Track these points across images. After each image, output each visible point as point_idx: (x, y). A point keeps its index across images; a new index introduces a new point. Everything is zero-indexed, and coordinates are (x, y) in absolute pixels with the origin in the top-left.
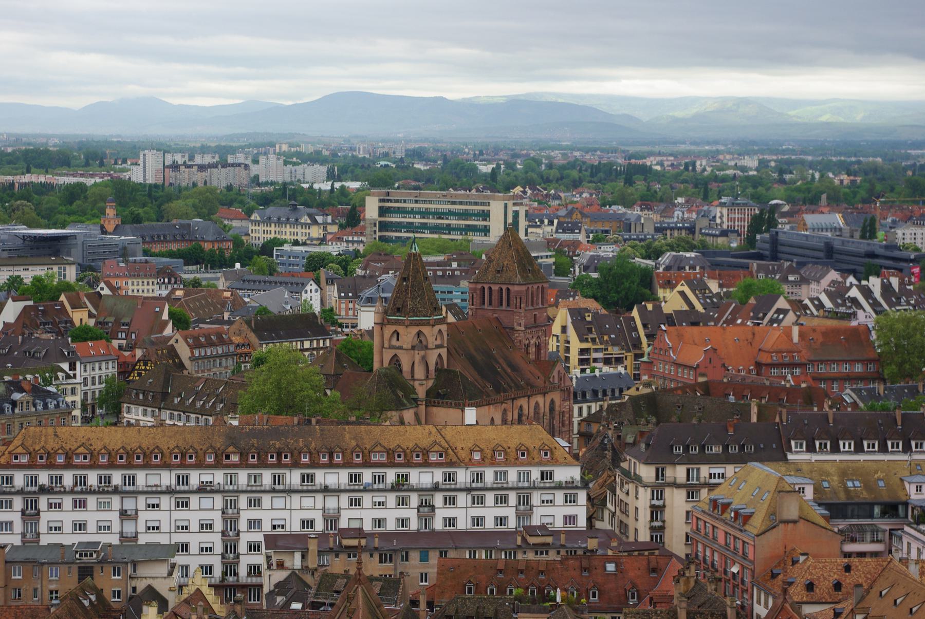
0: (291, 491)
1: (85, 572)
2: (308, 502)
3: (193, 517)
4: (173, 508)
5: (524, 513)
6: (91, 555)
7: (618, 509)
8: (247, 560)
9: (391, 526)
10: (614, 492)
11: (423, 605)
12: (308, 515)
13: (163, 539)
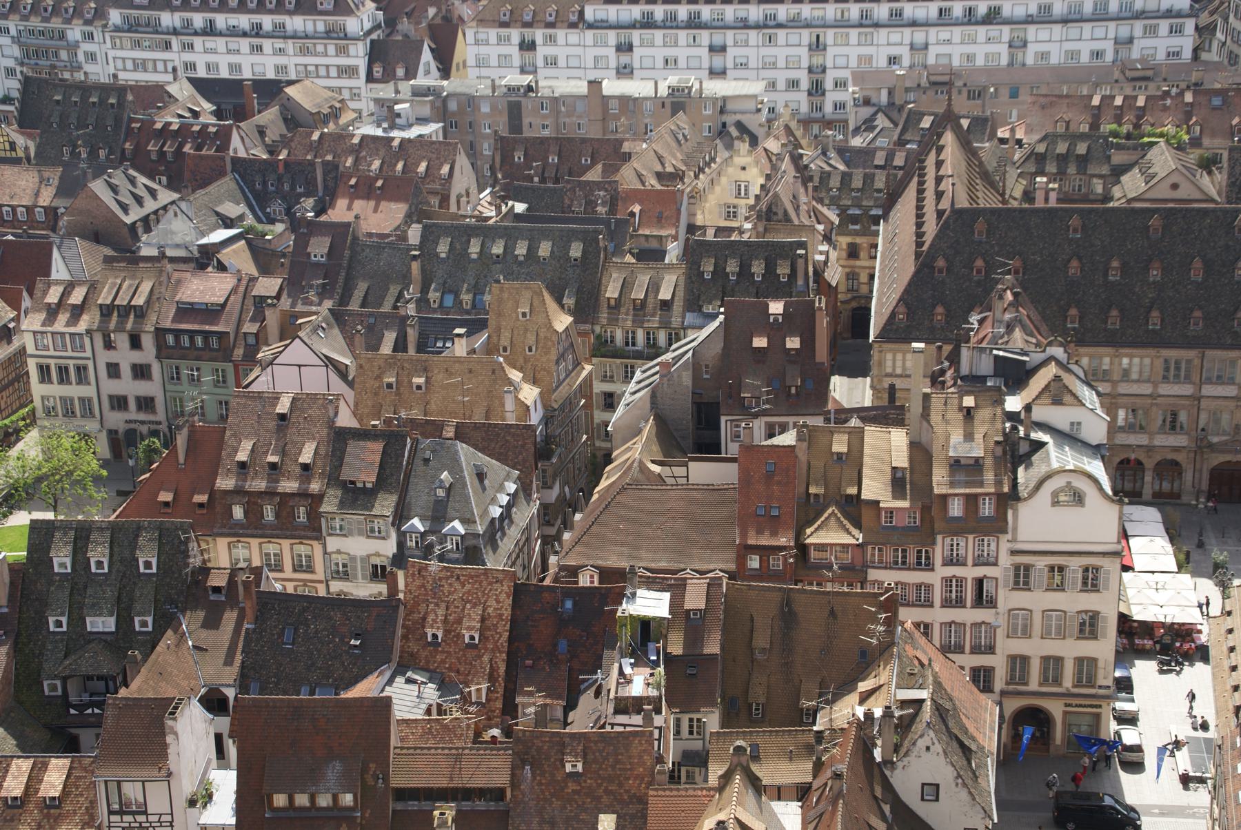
0: (877, 25)
2: (895, 35)
3: (780, 53)
4: (761, 44)
6: (683, 90)
7: (1229, 38)
8: (832, 97)
9: (980, 62)
10: (1226, 19)
11: (1011, 143)
12: (894, 51)
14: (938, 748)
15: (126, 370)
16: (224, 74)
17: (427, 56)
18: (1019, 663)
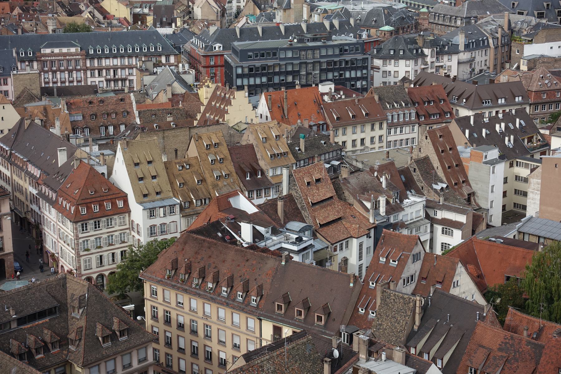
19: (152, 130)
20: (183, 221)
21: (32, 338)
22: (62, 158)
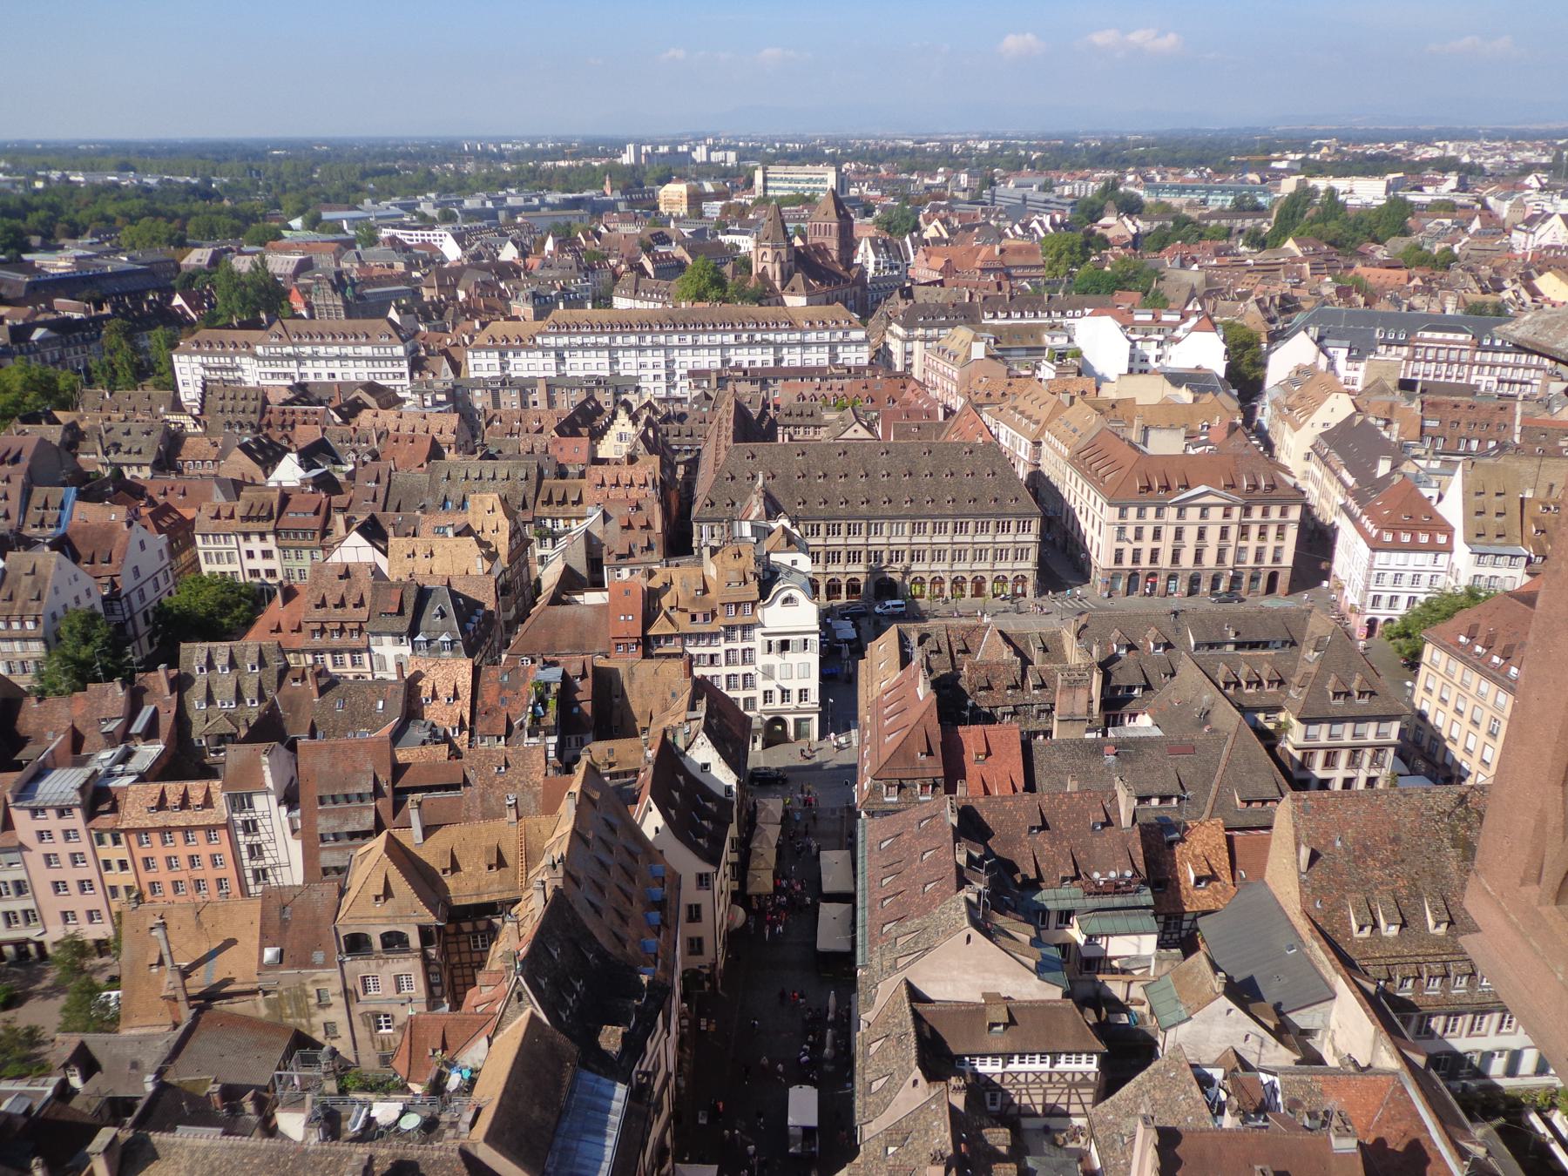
1: (590, 389)
3: (649, 358)
5: (834, 357)
9: (759, 365)
13: (634, 373)
14: (709, 743)
15: (258, 554)
16: (325, 378)
17: (446, 365)
18: (768, 695)
19: (1532, 454)
20: (1527, 579)
21: (1247, 668)
22: (1384, 467)
